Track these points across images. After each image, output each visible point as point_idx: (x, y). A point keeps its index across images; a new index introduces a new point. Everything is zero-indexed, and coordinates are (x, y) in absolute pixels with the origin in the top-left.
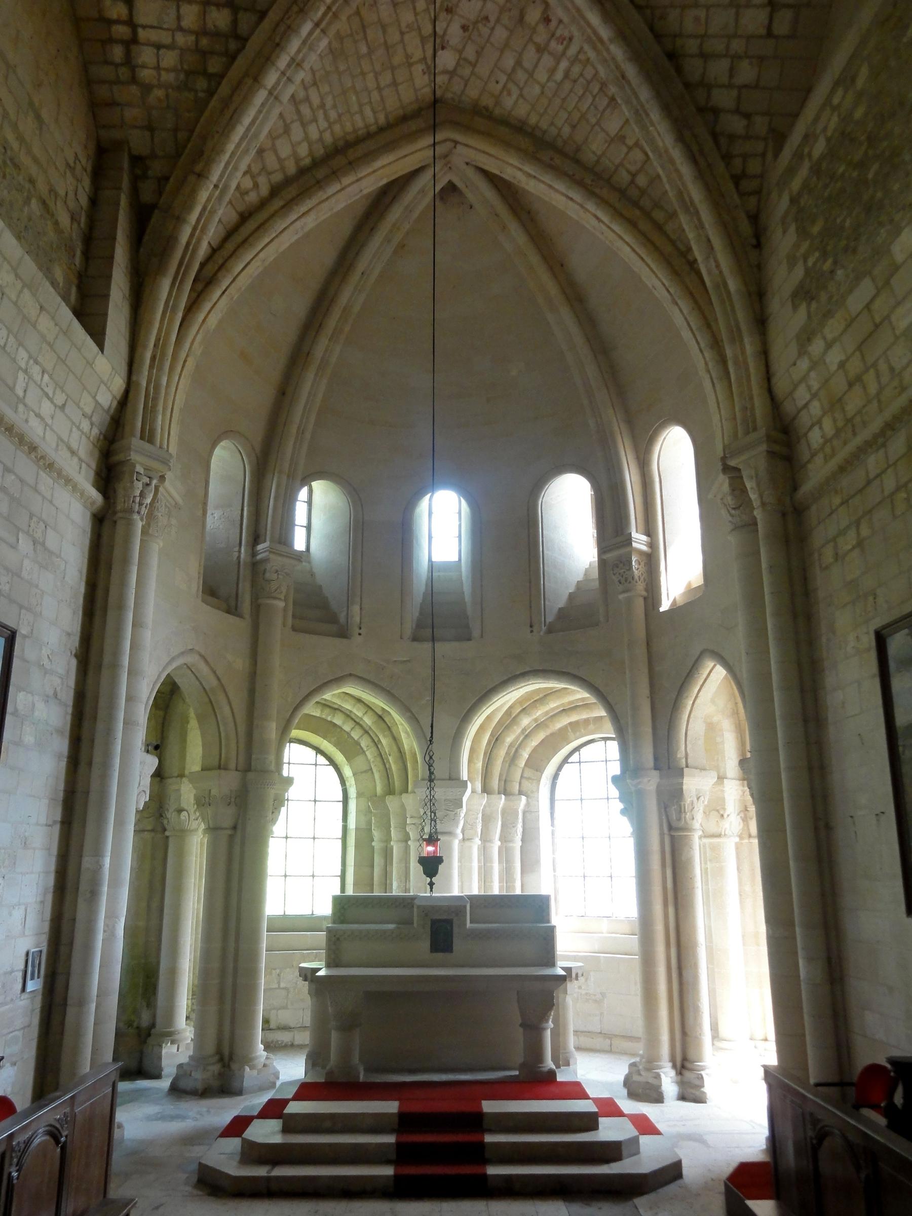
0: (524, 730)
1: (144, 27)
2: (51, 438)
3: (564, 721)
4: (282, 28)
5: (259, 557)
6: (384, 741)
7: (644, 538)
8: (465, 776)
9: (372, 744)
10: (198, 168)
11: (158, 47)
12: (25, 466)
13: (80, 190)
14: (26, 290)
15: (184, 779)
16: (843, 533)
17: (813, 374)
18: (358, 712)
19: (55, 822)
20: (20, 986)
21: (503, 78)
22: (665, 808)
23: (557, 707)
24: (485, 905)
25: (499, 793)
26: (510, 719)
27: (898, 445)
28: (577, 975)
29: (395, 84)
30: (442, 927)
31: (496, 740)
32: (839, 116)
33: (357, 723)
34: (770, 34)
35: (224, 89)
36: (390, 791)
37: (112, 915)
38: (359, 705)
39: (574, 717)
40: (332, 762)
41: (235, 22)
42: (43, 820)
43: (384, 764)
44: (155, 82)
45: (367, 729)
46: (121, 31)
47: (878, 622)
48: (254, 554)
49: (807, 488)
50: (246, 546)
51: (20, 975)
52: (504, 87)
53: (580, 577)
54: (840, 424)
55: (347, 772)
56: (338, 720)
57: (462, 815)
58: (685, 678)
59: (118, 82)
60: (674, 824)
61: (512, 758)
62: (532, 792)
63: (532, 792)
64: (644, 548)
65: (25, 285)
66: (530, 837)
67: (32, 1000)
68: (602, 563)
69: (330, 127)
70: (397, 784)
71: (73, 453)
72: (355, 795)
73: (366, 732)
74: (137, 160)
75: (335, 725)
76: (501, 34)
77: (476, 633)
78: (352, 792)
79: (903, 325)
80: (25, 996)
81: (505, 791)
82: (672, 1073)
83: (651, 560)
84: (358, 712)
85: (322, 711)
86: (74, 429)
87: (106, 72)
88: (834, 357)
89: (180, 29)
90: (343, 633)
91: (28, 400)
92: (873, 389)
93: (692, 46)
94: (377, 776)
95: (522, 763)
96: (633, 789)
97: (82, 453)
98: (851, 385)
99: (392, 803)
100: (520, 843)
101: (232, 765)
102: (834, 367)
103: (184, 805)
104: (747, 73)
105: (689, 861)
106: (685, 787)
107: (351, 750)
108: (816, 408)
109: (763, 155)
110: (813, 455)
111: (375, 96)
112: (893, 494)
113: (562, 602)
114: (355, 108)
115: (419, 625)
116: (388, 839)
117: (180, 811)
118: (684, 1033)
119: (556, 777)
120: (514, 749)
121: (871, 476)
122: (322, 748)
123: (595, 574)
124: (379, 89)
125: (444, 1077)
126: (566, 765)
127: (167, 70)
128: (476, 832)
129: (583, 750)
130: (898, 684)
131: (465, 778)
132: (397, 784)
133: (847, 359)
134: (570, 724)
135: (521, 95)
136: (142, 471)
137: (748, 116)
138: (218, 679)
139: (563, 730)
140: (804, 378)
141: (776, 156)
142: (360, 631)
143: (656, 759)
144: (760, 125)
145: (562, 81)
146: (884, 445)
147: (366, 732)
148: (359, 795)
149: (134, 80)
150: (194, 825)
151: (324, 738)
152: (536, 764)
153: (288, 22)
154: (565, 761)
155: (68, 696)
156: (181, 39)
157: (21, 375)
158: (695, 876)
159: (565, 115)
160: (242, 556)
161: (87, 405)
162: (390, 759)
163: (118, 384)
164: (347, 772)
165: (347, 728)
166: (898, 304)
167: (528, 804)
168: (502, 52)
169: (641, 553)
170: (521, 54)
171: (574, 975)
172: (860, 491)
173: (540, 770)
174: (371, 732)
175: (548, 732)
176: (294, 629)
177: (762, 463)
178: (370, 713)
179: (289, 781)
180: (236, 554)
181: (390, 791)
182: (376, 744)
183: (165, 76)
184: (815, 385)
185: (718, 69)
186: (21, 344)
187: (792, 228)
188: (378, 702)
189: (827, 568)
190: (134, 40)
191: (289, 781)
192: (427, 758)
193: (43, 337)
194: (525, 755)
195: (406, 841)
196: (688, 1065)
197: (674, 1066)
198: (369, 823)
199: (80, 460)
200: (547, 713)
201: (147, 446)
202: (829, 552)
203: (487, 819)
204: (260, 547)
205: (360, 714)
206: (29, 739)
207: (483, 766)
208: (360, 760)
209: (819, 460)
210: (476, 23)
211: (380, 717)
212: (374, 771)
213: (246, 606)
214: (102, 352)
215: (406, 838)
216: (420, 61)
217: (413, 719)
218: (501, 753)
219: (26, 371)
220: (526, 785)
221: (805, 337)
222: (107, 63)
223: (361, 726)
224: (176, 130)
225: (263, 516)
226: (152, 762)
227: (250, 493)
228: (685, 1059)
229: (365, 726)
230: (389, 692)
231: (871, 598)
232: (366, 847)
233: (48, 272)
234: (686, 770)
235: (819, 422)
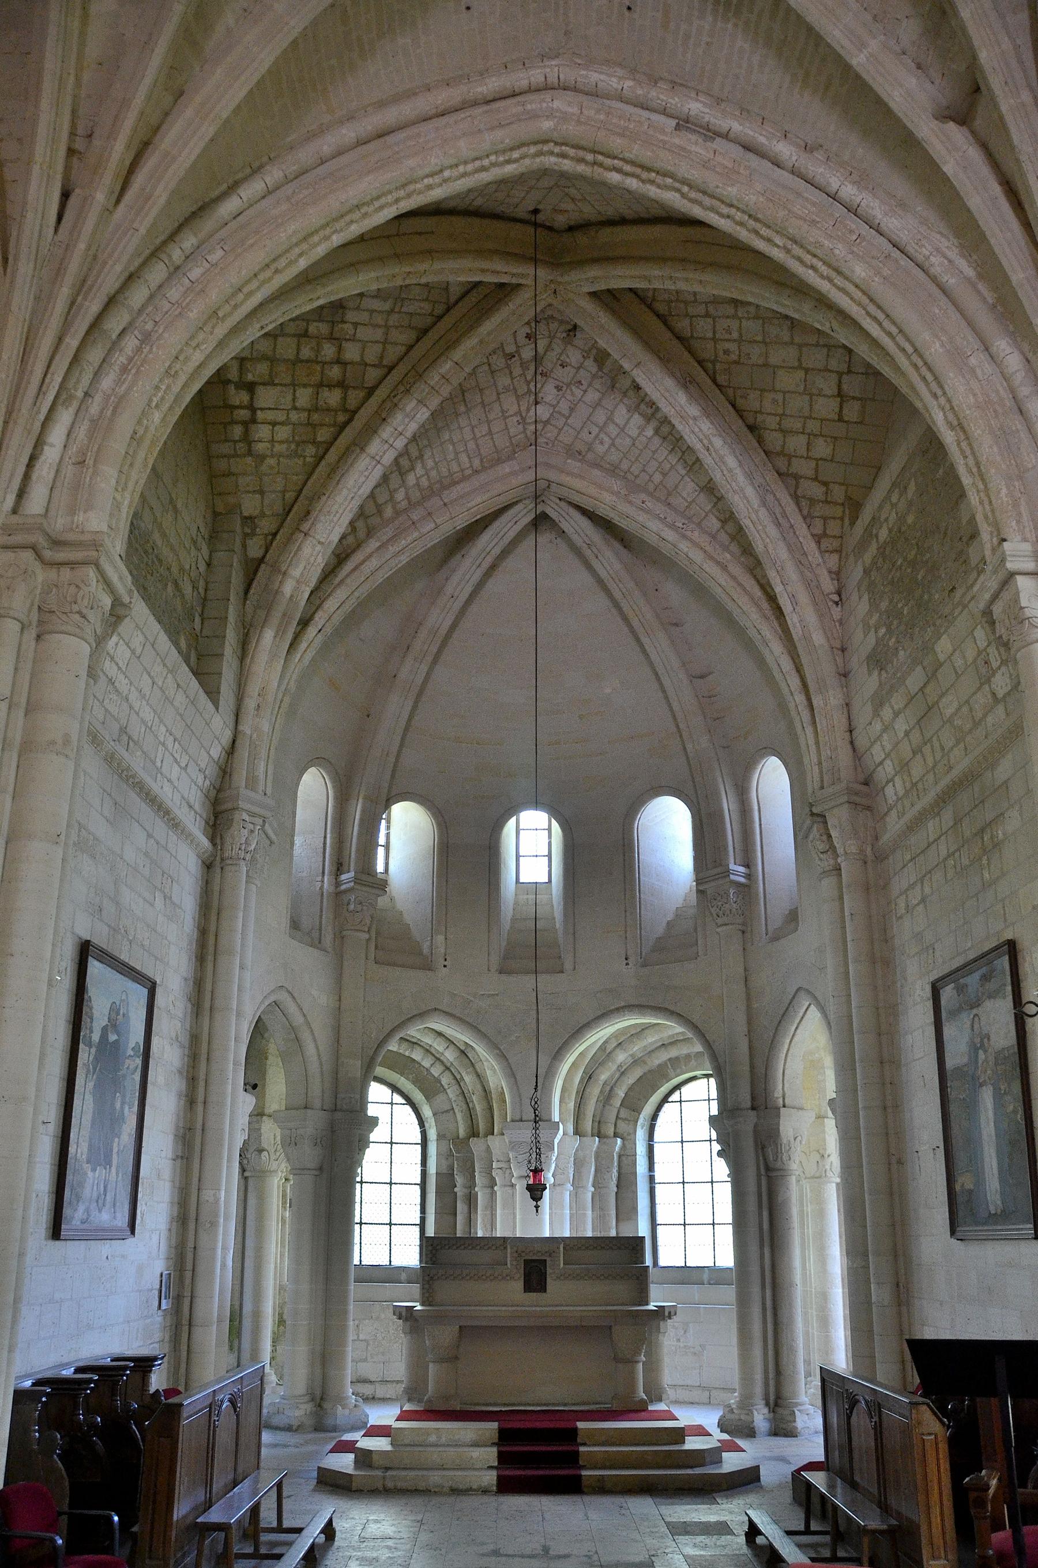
0: (620, 1066)
1: (262, 409)
2: (177, 798)
3: (663, 1056)
4: (388, 405)
5: (343, 887)
6: (468, 1079)
7: (742, 869)
8: (556, 1118)
9: (454, 1082)
10: (305, 526)
11: (274, 424)
12: (160, 829)
13: (200, 558)
14: (169, 675)
15: (264, 1118)
16: (912, 886)
17: (885, 736)
18: (439, 1046)
19: (177, 1156)
20: (157, 1304)
21: (595, 430)
22: (763, 1148)
23: (655, 1042)
25: (592, 1136)
26: (604, 1054)
27: (947, 816)
28: (670, 1313)
29: (490, 433)
31: (589, 1078)
32: (897, 514)
34: (840, 419)
35: (332, 456)
36: (474, 1133)
37: (224, 1248)
38: (439, 1039)
39: (674, 1052)
40: (410, 1102)
41: (344, 399)
42: (170, 1155)
44: (269, 453)
45: (448, 1065)
46: (243, 414)
47: (935, 975)
48: (338, 884)
49: (886, 838)
50: (330, 874)
51: (157, 1293)
52: (597, 436)
53: (680, 903)
54: (908, 785)
55: (427, 1112)
56: (417, 1055)
57: (554, 1158)
58: (784, 1015)
59: (236, 455)
60: (771, 1166)
62: (629, 1134)
63: (629, 1134)
64: (742, 880)
65: (171, 672)
66: (626, 1182)
67: (165, 1316)
69: (427, 474)
70: (482, 1126)
71: (190, 807)
72: (435, 1137)
74: (249, 520)
76: (592, 396)
77: (568, 966)
78: (432, 1134)
79: (948, 712)
80: (160, 1313)
82: (766, 1411)
84: (439, 1046)
85: (399, 1045)
86: (193, 786)
87: (226, 448)
88: (901, 726)
89: (295, 408)
90: (427, 965)
91: (164, 770)
92: (930, 762)
93: (772, 422)
94: (459, 1116)
96: (730, 1130)
97: (197, 807)
98: (914, 753)
99: (477, 1146)
100: (615, 1189)
101: (317, 1103)
102: (901, 735)
103: (265, 1145)
104: (822, 448)
105: (786, 1202)
106: (781, 1128)
107: (431, 1088)
108: (889, 767)
109: (842, 519)
110: (890, 810)
111: (471, 445)
112: (946, 859)
113: (660, 930)
114: (452, 456)
117: (260, 1151)
118: (778, 1373)
119: (654, 1117)
120: (608, 1088)
121: (931, 840)
122: (399, 1085)
123: (694, 896)
124: (475, 438)
125: (539, 1408)
126: (666, 1105)
127: (281, 442)
128: (568, 1177)
129: (684, 1089)
130: (948, 1031)
131: (557, 1119)
133: (911, 730)
134: (670, 1059)
135: (613, 444)
136: (247, 818)
137: (825, 484)
138: (304, 1016)
139: (662, 1067)
140: (879, 738)
141: (852, 524)
142: (446, 963)
143: (753, 1098)
144: (838, 493)
145: (652, 437)
146: (938, 814)
147: (448, 1068)
148: (440, 1137)
149: (250, 453)
150: (274, 1166)
152: (633, 1104)
153: (395, 400)
154: (665, 1100)
155: (185, 1039)
156: (294, 416)
157: (160, 747)
158: (791, 1217)
159: (656, 464)
160: (326, 886)
161: (204, 761)
162: (474, 1098)
163: (228, 734)
165: (426, 1063)
166: (943, 695)
167: (624, 1147)
168: (594, 408)
169: (738, 884)
170: (612, 413)
171: (667, 1314)
172: (923, 852)
173: (637, 1110)
175: (646, 1068)
178: (452, 1047)
179: (374, 1122)
180: (319, 884)
181: (474, 1133)
183: (278, 448)
184: (888, 747)
185: (797, 443)
186: (161, 721)
187: (866, 597)
188: (462, 1036)
189: (901, 917)
190: (254, 421)
191: (374, 1122)
192: (533, 1103)
193: (177, 709)
194: (621, 1093)
195: (492, 1187)
196: (779, 1401)
197: (767, 1404)
199: (196, 812)
201: (252, 794)
202: (902, 905)
203: (579, 1164)
204: (343, 877)
205: (441, 1049)
206: (161, 1080)
208: (441, 1098)
209: (894, 813)
210: (568, 385)
212: (456, 1111)
213: (328, 940)
214: (217, 709)
215: (492, 1183)
216: (515, 414)
217: (502, 1056)
218: (595, 1092)
219: (163, 744)
221: (878, 702)
222: (226, 441)
223: (442, 1062)
224: (284, 492)
226: (247, 1102)
227: (333, 818)
228: (778, 1397)
229: (445, 1060)
230: (475, 1027)
231: (931, 951)
233: (176, 644)
234: (782, 1110)
235: (892, 780)
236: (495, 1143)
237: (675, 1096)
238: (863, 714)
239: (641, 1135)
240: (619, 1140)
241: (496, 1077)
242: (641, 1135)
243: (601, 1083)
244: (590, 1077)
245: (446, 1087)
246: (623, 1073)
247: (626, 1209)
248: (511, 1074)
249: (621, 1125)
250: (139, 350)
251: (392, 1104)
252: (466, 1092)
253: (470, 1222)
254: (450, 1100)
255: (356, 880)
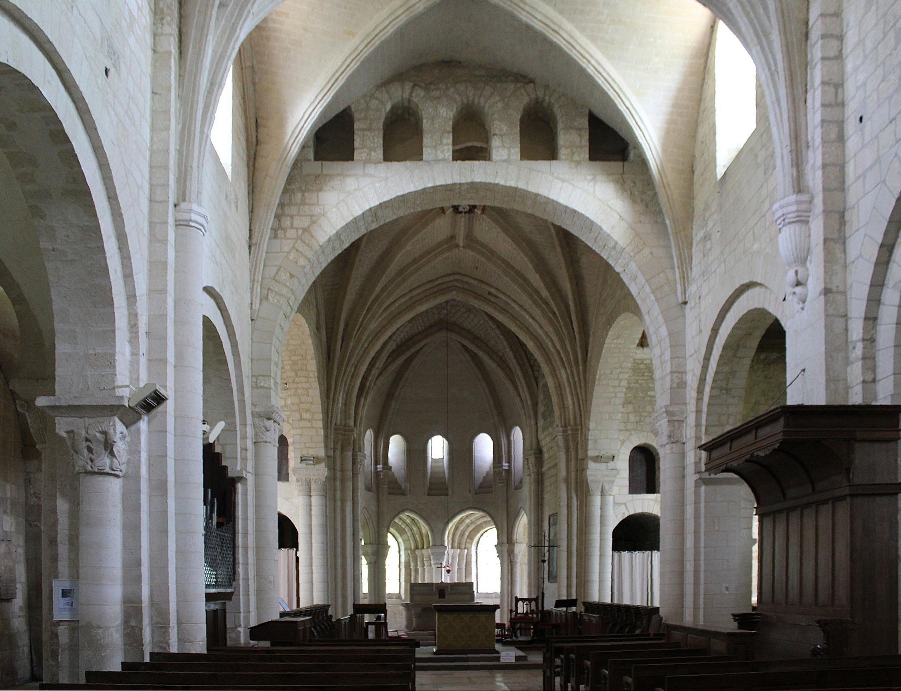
24: (453, 585)
30: (442, 590)
31: (456, 528)
36: (417, 548)
48: (376, 468)
58: (517, 515)
61: (462, 535)
66: (468, 564)
68: (494, 472)
70: (420, 545)
77: (450, 493)
81: (459, 548)
83: (508, 471)
88: (548, 439)
95: (465, 537)
99: (418, 552)
107: (402, 532)
113: (481, 479)
115: (430, 489)
116: (416, 565)
132: (420, 545)
148: (406, 549)
152: (471, 537)
164: (400, 540)
173: (472, 540)
176: (389, 494)
177: (533, 459)
181: (417, 548)
182: (412, 530)
188: (413, 516)
194: (467, 534)
208: (405, 536)
211: (413, 520)
213: (374, 488)
217: (429, 524)
218: (458, 533)
221: (543, 430)
225: (381, 456)
232: (409, 569)
236: (425, 552)
238: (540, 430)
239: (473, 548)
241: (425, 528)
242: (473, 548)
247: (468, 573)
248: (432, 530)
249: (467, 545)
250: (355, 371)
253: (416, 578)
255: (384, 468)
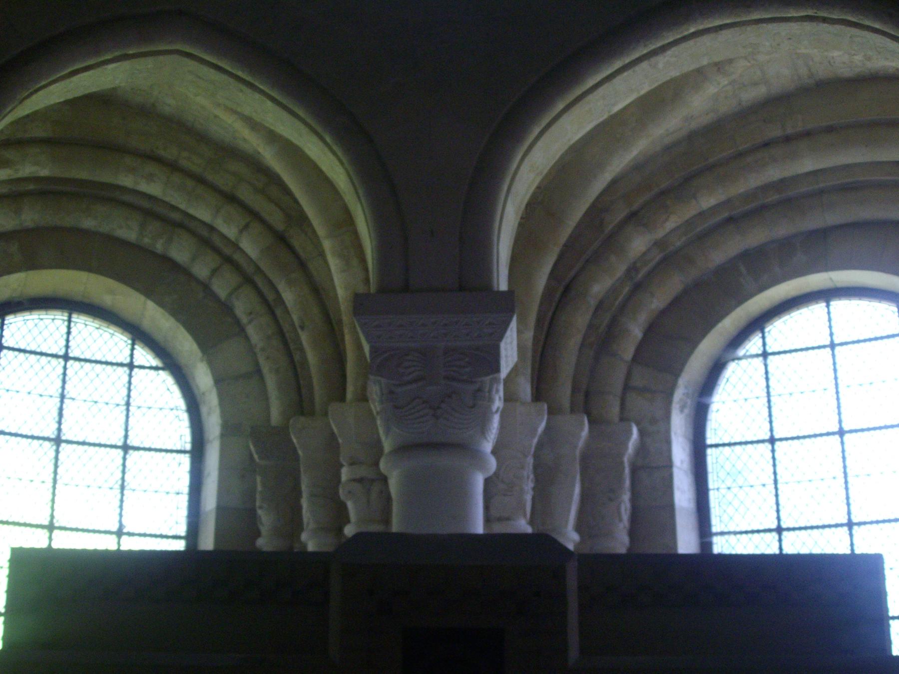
0: (633, 269)
23: (714, 210)
33: (228, 258)
39: (756, 236)
43: (290, 356)
45: (250, 270)
56: (181, 251)
61: (603, 340)
63: (654, 421)
73: (248, 280)
75: (175, 266)
95: (628, 350)
120: (606, 318)
122: (146, 325)
128: (521, 505)
134: (746, 256)
148: (229, 430)
151: (148, 292)
162: (304, 337)
164: (203, 378)
165: (201, 270)
167: (642, 449)
174: (259, 280)
182: (271, 306)
194: (636, 331)
198: (250, 495)
200: (689, 224)
205: (230, 231)
207: (536, 338)
212: (265, 370)
220: (637, 403)
237: (753, 345)
240: (635, 431)
243: (593, 303)
244: (567, 289)
245: (244, 320)
246: (638, 287)
251: (131, 366)
252: (286, 328)
254: (251, 349)
